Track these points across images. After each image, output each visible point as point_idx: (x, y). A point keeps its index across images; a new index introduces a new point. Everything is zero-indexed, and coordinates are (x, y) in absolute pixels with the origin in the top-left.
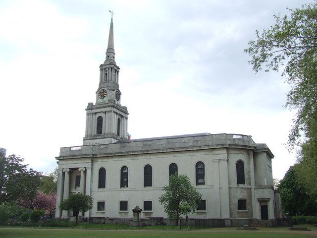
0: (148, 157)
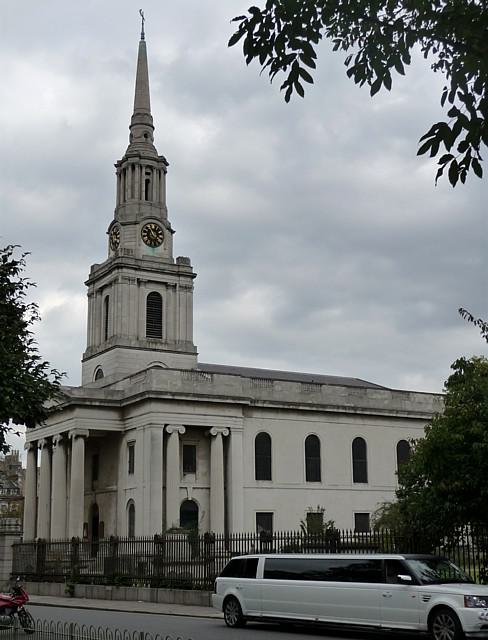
0: (359, 421)
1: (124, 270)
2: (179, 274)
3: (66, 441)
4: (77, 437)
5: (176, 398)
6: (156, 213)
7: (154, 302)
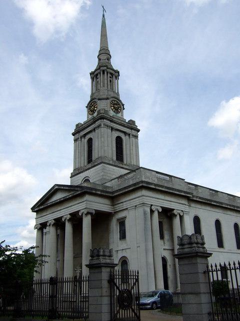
1: (105, 120)
2: (132, 129)
3: (76, 219)
4: (86, 214)
5: (157, 188)
6: (116, 96)
7: (119, 141)
